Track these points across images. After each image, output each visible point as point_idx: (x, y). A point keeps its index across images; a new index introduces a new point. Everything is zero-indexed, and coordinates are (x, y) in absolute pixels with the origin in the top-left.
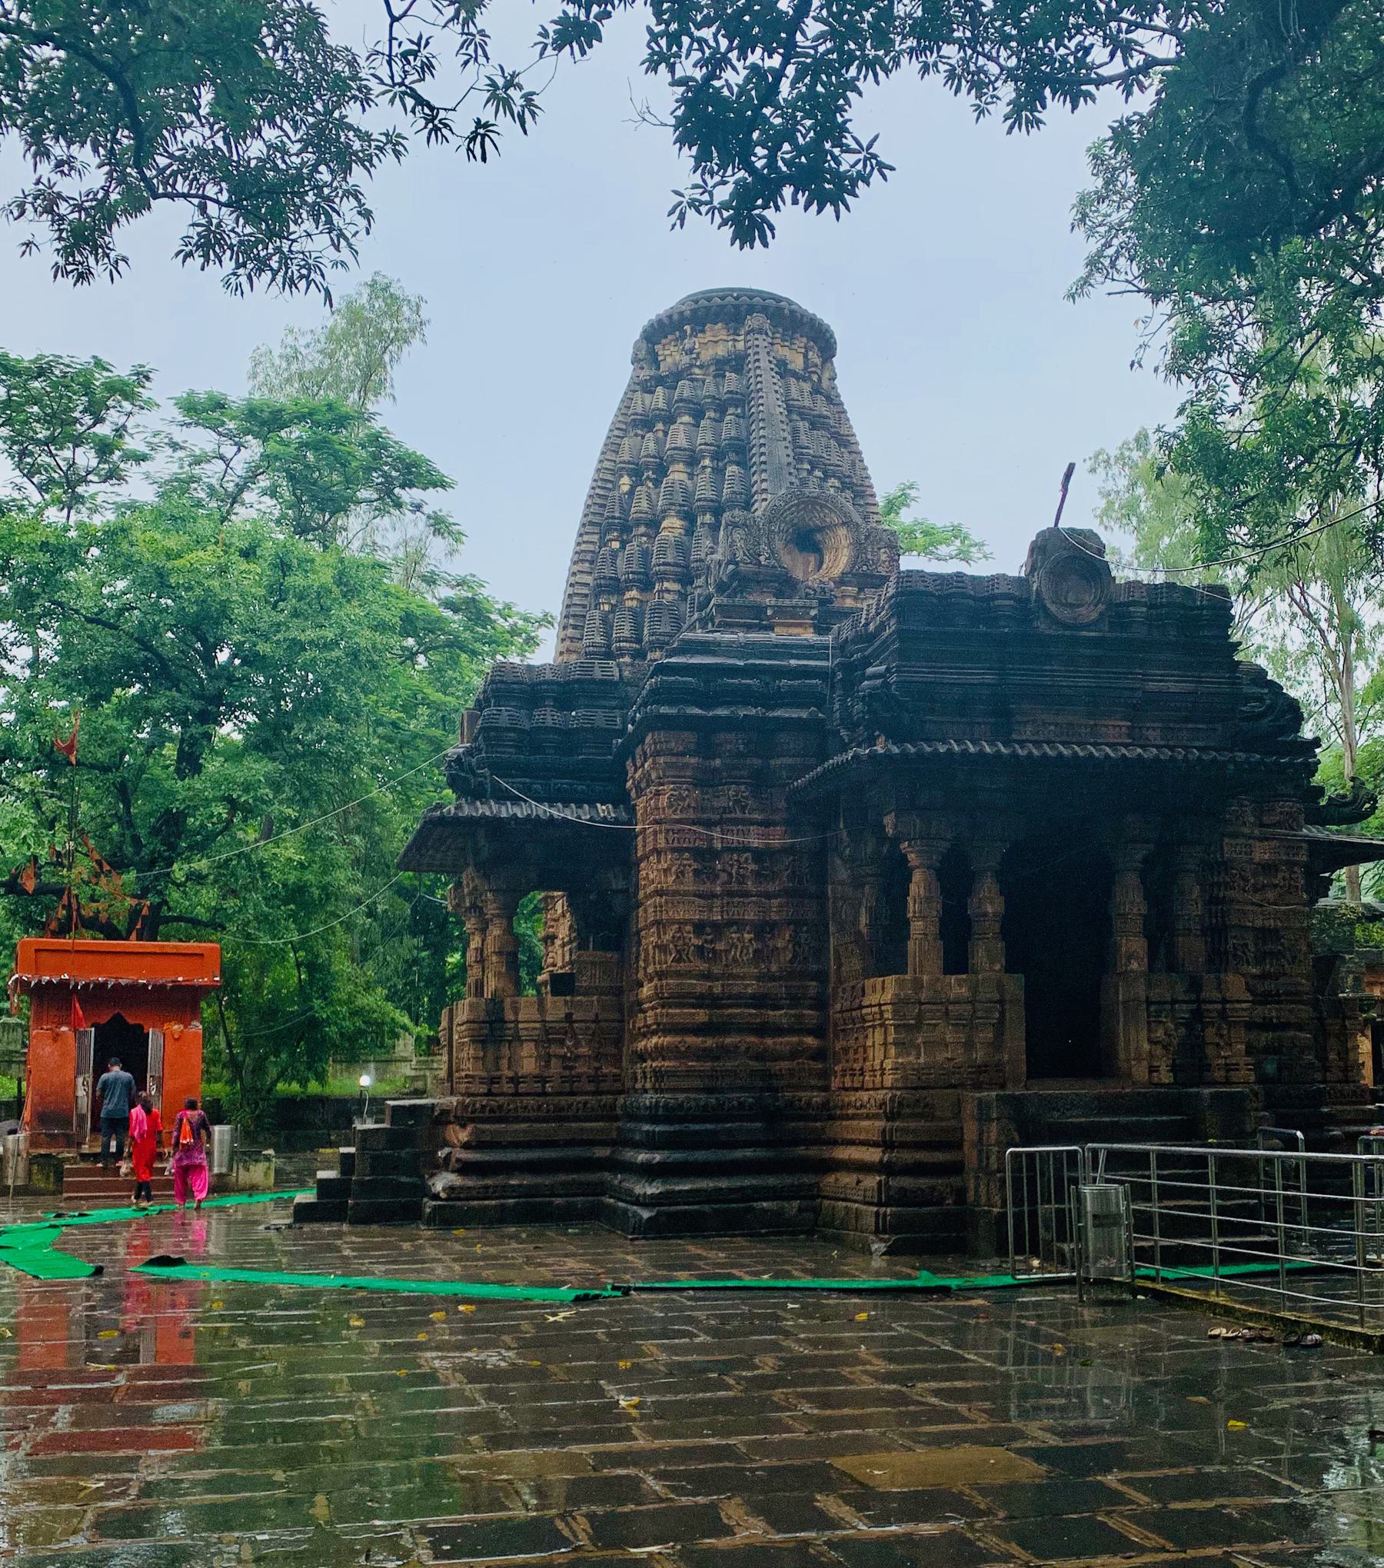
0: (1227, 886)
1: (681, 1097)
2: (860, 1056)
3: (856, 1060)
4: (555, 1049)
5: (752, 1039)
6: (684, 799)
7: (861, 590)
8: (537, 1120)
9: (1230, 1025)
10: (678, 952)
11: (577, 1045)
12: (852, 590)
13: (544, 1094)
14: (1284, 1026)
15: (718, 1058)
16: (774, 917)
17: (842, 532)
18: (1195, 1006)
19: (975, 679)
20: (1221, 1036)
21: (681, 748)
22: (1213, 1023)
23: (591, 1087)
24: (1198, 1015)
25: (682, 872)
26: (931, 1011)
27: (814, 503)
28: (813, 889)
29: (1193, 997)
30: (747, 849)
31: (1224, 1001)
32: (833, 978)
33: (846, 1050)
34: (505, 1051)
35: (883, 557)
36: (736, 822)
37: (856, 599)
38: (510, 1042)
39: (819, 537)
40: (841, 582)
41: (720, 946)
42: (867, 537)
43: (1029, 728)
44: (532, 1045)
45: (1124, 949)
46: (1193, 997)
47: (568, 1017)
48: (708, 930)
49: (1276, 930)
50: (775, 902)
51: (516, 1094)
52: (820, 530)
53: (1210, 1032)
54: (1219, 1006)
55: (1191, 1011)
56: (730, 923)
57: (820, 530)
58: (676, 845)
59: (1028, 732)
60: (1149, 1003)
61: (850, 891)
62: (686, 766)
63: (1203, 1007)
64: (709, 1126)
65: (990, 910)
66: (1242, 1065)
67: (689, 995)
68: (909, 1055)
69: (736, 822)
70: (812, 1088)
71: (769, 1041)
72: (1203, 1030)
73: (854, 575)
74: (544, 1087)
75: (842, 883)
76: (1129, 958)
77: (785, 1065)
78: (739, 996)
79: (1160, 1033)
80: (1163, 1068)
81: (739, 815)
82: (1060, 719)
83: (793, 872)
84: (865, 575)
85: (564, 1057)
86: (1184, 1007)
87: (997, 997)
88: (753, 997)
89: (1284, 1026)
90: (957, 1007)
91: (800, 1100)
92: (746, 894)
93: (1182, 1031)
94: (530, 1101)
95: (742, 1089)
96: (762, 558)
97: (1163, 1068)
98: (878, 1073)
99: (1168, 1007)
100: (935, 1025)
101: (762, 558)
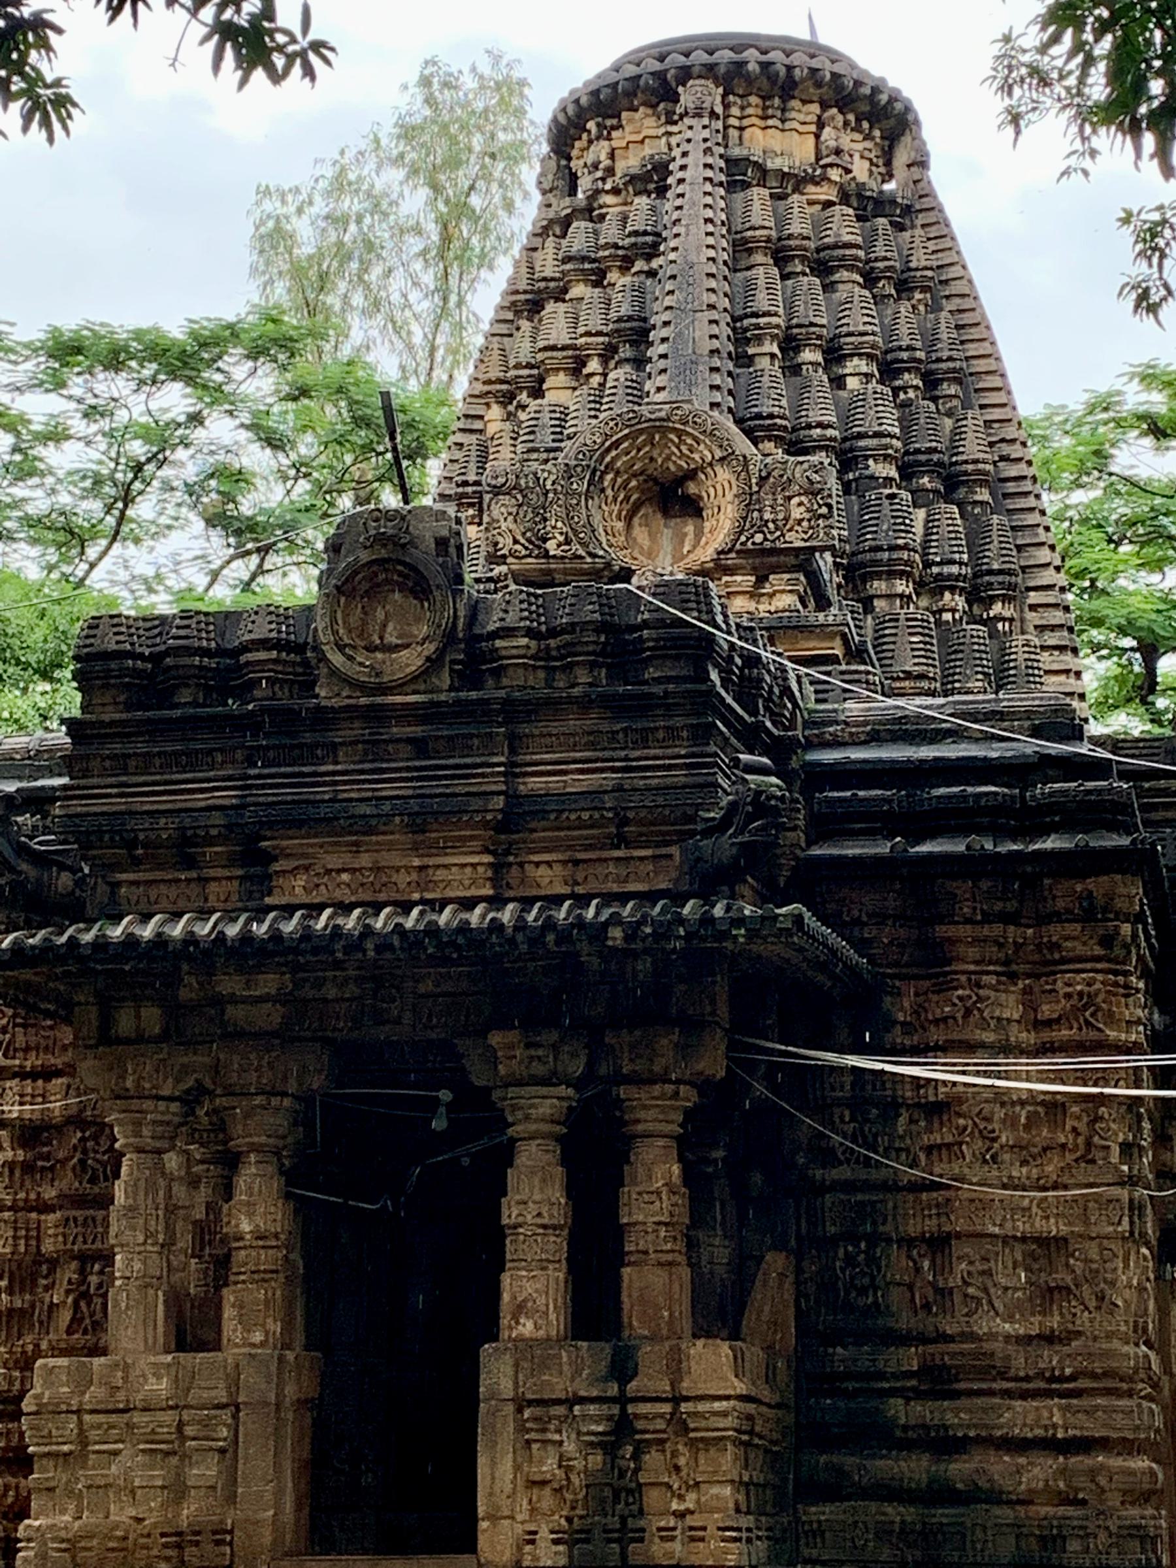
0: (951, 1149)
7: (761, 580)
9: (692, 1443)
12: (745, 581)
14: (1084, 1445)
16: (48, 1246)
17: (723, 474)
18: (616, 1410)
19: (200, 800)
20: (677, 1468)
22: (662, 1442)
24: (623, 1428)
26: (99, 1426)
27: (659, 429)
29: (613, 1390)
31: (677, 1400)
35: (797, 513)
37: (754, 595)
39: (692, 488)
40: (719, 568)
42: (762, 480)
43: (300, 881)
45: (506, 1297)
46: (613, 1390)
49: (1061, 1242)
50: (52, 1218)
52: (691, 475)
53: (653, 1458)
54: (666, 1408)
55: (610, 1418)
57: (691, 475)
59: (297, 888)
60: (521, 1404)
63: (630, 1409)
65: (246, 1227)
66: (711, 1529)
68: (63, 1512)
72: (636, 1457)
73: (738, 552)
76: (520, 1309)
79: (549, 1466)
80: (544, 1534)
82: (365, 860)
83: (82, 1162)
84: (762, 552)
86: (592, 1409)
87: (222, 1396)
89: (1084, 1445)
90: (147, 1417)
93: (597, 1460)
96: (551, 545)
97: (544, 1534)
99: (560, 1410)
100: (116, 1453)
101: (551, 545)
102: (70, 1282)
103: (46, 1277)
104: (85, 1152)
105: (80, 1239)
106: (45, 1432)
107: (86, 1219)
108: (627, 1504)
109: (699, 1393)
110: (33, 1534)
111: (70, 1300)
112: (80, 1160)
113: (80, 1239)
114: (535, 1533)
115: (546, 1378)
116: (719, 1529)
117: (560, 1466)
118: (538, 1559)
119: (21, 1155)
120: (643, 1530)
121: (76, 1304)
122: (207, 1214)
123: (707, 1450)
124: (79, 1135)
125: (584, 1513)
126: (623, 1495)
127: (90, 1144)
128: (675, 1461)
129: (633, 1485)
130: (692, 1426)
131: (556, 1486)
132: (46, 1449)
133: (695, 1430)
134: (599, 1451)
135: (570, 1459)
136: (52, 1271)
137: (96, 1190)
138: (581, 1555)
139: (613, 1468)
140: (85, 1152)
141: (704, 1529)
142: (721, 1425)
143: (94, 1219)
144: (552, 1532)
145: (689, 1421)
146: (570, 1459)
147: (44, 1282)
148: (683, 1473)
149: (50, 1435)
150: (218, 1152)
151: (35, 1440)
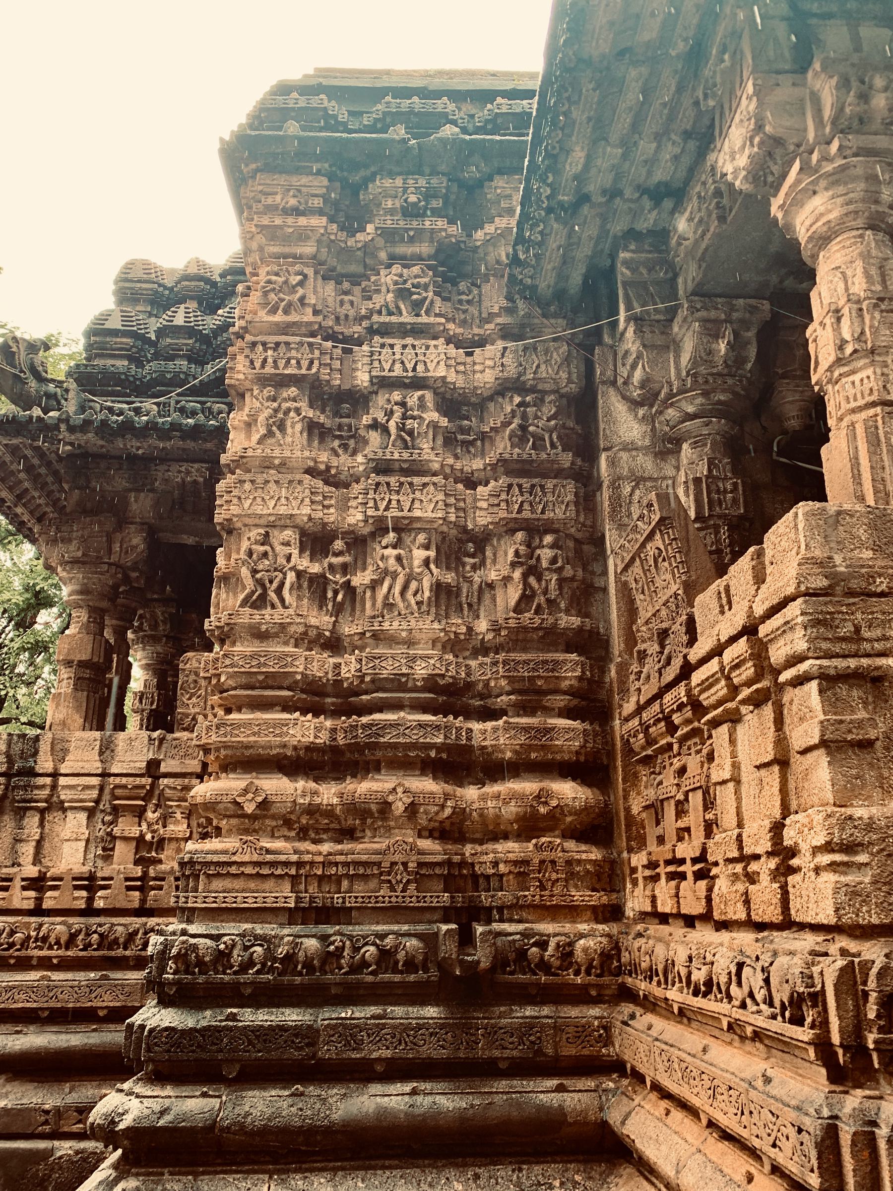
1: (231, 929)
2: (694, 818)
3: (683, 833)
4: (127, 827)
5: (427, 785)
6: (293, 289)
8: (65, 965)
10: (260, 583)
11: (165, 819)
13: (89, 911)
15: (348, 834)
21: (293, 202)
23: (79, 898)
25: (282, 427)
28: (566, 459)
30: (418, 383)
32: (617, 645)
33: (656, 809)
34: (32, 822)
36: (404, 331)
38: (42, 812)
41: (360, 579)
44: (83, 816)
47: (152, 768)
48: (338, 545)
51: (38, 911)
56: (380, 528)
58: (269, 370)
61: (646, 463)
62: (302, 236)
64: (292, 1016)
67: (272, 681)
69: (404, 331)
70: (572, 912)
71: (471, 793)
74: (90, 900)
75: (628, 447)
77: (510, 849)
78: (398, 683)
81: (407, 318)
83: (523, 428)
85: (140, 840)
88: (431, 683)
91: (543, 945)
92: (414, 469)
94: (58, 927)
95: (395, 912)
98: (765, 867)
102: (517, 553)
103: (473, 556)
104: (524, 417)
105: (526, 506)
106: (847, 629)
107: (533, 486)
110: (859, 836)
111: (517, 574)
112: (520, 426)
113: (526, 506)
119: (444, 422)
121: (525, 576)
122: (710, 470)
124: (517, 399)
127: (531, 410)
132: (852, 663)
136: (480, 550)
137: (544, 456)
140: (524, 417)
143: (542, 487)
147: (472, 561)
149: (857, 636)
150: (720, 402)
151: (825, 645)
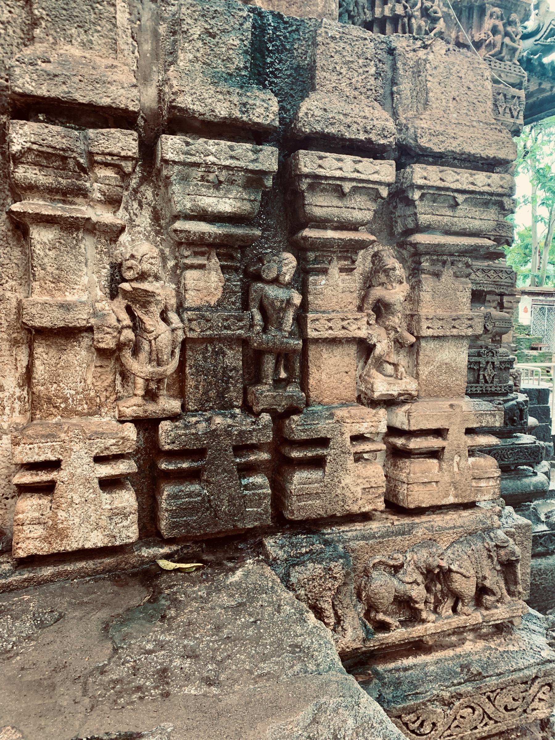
108: (278, 383)
109: (453, 146)
114: (55, 465)
115: (75, 51)
116: (469, 431)
117: (113, 294)
118: (62, 534)
120: (324, 442)
123: (437, 275)
125: (175, 405)
126: (269, 364)
128: (377, 292)
129: (298, 343)
130: (424, 219)
131: (108, 342)
133: (428, 229)
134: (215, 262)
135: (143, 276)
138: (173, 513)
139: (246, 306)
141: (439, 433)
142: (476, 224)
144: (99, 460)
145: (421, 207)
146: (143, 276)
148: (396, 320)
